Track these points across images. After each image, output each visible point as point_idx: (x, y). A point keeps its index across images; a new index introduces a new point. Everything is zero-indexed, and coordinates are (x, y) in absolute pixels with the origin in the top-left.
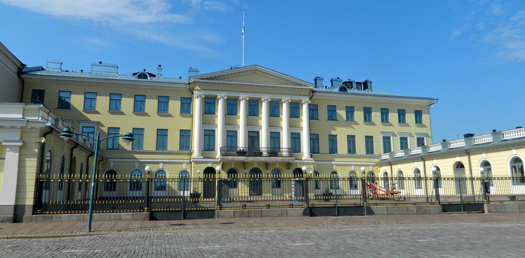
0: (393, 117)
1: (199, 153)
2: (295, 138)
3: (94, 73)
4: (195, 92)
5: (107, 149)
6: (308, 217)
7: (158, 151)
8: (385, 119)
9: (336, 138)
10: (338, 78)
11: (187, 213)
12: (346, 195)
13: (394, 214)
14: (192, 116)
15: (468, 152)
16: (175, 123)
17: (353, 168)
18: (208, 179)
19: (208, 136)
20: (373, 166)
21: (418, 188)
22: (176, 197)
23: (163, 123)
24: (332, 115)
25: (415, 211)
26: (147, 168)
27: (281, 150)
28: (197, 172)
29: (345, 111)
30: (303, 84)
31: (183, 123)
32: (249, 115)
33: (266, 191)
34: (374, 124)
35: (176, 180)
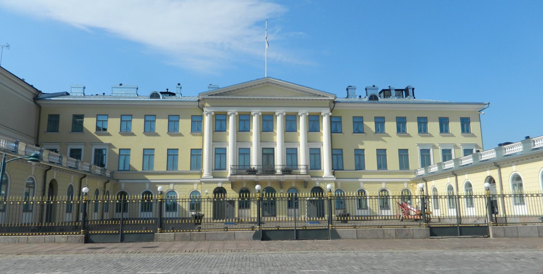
0: (433, 127)
1: (209, 172)
3: (114, 95)
4: (205, 109)
5: (119, 170)
7: (168, 172)
8: (423, 129)
9: (364, 152)
10: (374, 86)
11: (126, 236)
12: (376, 216)
13: (366, 238)
14: (202, 135)
15: (497, 165)
16: (185, 142)
17: (383, 186)
18: (218, 199)
19: (219, 154)
20: (408, 183)
21: (470, 207)
22: (187, 218)
23: (173, 142)
24: (358, 126)
25: (393, 235)
26: (159, 188)
27: (299, 167)
28: (207, 192)
29: (374, 123)
30: (322, 95)
31: (194, 142)
32: (310, 131)
33: (281, 212)
34: (409, 136)
35: (187, 200)
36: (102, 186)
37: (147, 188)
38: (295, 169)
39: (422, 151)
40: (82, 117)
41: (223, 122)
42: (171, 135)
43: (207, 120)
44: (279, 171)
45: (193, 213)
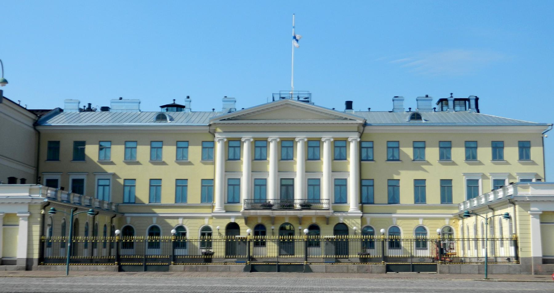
0: (485, 153)
1: (221, 206)
2: (340, 187)
4: (217, 135)
6: (249, 273)
8: (471, 157)
10: (427, 96)
14: (214, 164)
17: (420, 222)
19: (233, 186)
20: (451, 219)
23: (182, 172)
25: (356, 270)
28: (219, 228)
34: (454, 164)
36: (109, 221)
37: (155, 222)
38: (317, 203)
39: (469, 181)
40: (83, 143)
41: (237, 149)
42: (180, 164)
43: (219, 147)
44: (298, 206)
45: (204, 251)
